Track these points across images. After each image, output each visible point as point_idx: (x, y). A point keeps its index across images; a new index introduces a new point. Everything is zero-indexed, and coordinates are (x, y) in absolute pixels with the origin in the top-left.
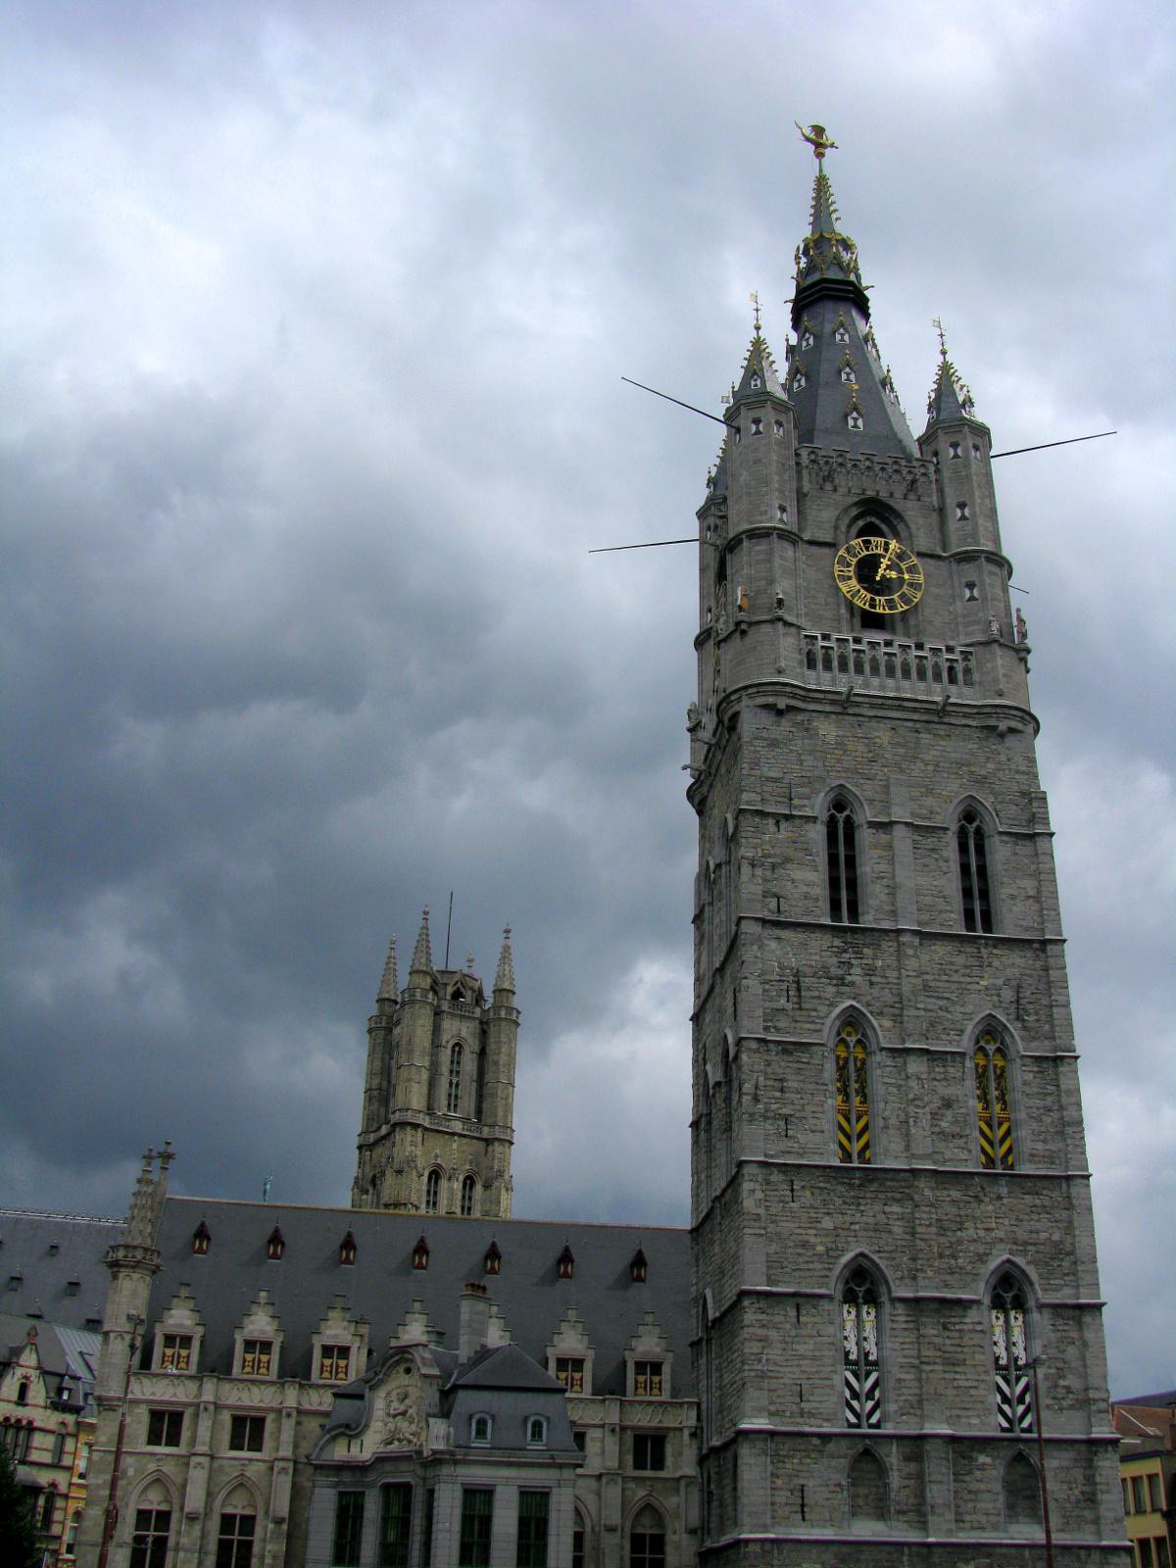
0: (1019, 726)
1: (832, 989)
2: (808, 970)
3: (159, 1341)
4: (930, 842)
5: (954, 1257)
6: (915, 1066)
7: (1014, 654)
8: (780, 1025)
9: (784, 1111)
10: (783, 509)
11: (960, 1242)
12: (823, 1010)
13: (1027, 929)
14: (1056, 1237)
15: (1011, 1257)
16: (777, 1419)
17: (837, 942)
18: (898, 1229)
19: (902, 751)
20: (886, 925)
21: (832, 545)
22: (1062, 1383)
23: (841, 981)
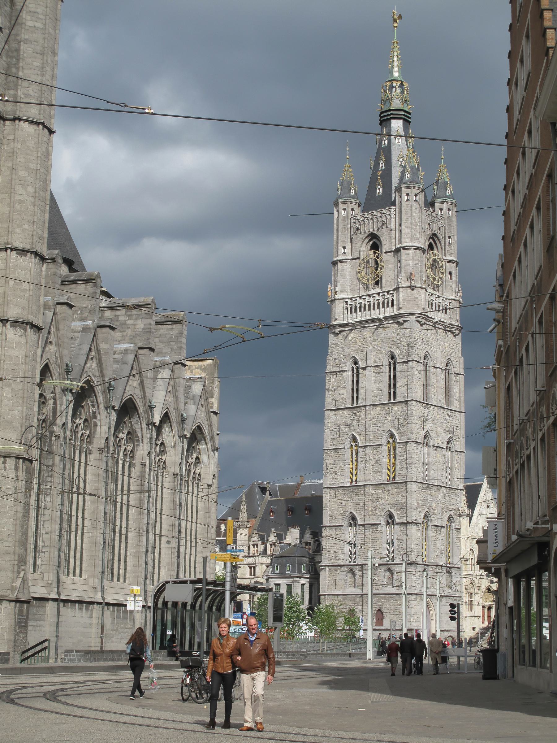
0: (408, 319)
1: (348, 429)
2: (342, 424)
3: (251, 547)
4: (379, 371)
5: (375, 510)
6: (368, 450)
7: (409, 288)
8: (334, 443)
9: (335, 471)
10: (344, 248)
11: (377, 506)
12: (345, 436)
13: (404, 397)
14: (403, 502)
15: (390, 509)
16: (330, 562)
17: (350, 413)
18: (361, 504)
19: (372, 338)
20: (364, 404)
21: (358, 258)
22: (401, 546)
23: (351, 426)
